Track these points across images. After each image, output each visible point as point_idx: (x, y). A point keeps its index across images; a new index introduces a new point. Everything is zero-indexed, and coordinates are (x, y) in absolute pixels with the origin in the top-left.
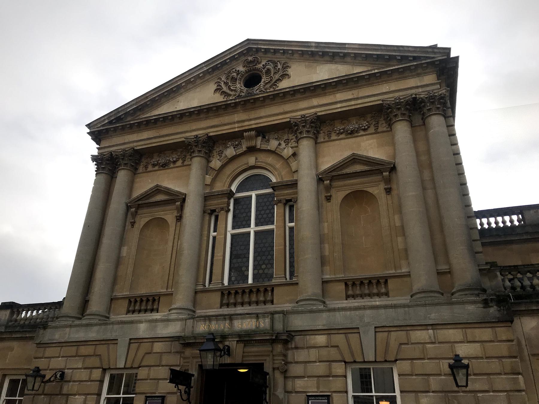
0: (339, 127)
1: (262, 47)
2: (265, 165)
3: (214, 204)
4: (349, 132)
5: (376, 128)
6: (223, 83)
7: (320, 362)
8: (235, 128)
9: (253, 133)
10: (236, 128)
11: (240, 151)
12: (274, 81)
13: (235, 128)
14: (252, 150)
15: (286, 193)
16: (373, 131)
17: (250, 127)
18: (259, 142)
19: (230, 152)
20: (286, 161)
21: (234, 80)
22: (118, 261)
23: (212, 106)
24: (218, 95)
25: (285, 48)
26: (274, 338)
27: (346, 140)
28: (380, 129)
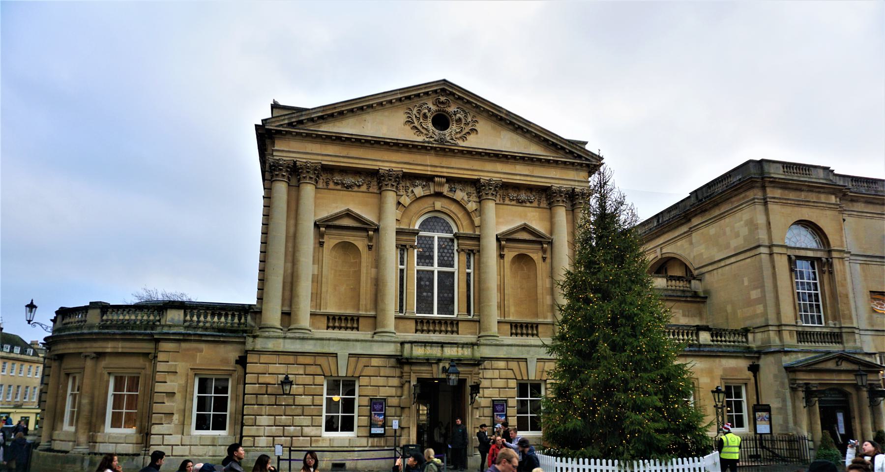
0: (513, 194)
1: (457, 93)
6: (414, 117)
8: (428, 171)
9: (444, 180)
10: (429, 171)
11: (427, 192)
12: (464, 132)
13: (428, 171)
14: (439, 195)
15: (469, 244)
16: (537, 206)
17: (442, 174)
18: (445, 190)
19: (419, 191)
20: (468, 214)
21: (425, 116)
23: (409, 143)
24: (408, 127)
25: (478, 104)
27: (517, 207)
28: (542, 205)
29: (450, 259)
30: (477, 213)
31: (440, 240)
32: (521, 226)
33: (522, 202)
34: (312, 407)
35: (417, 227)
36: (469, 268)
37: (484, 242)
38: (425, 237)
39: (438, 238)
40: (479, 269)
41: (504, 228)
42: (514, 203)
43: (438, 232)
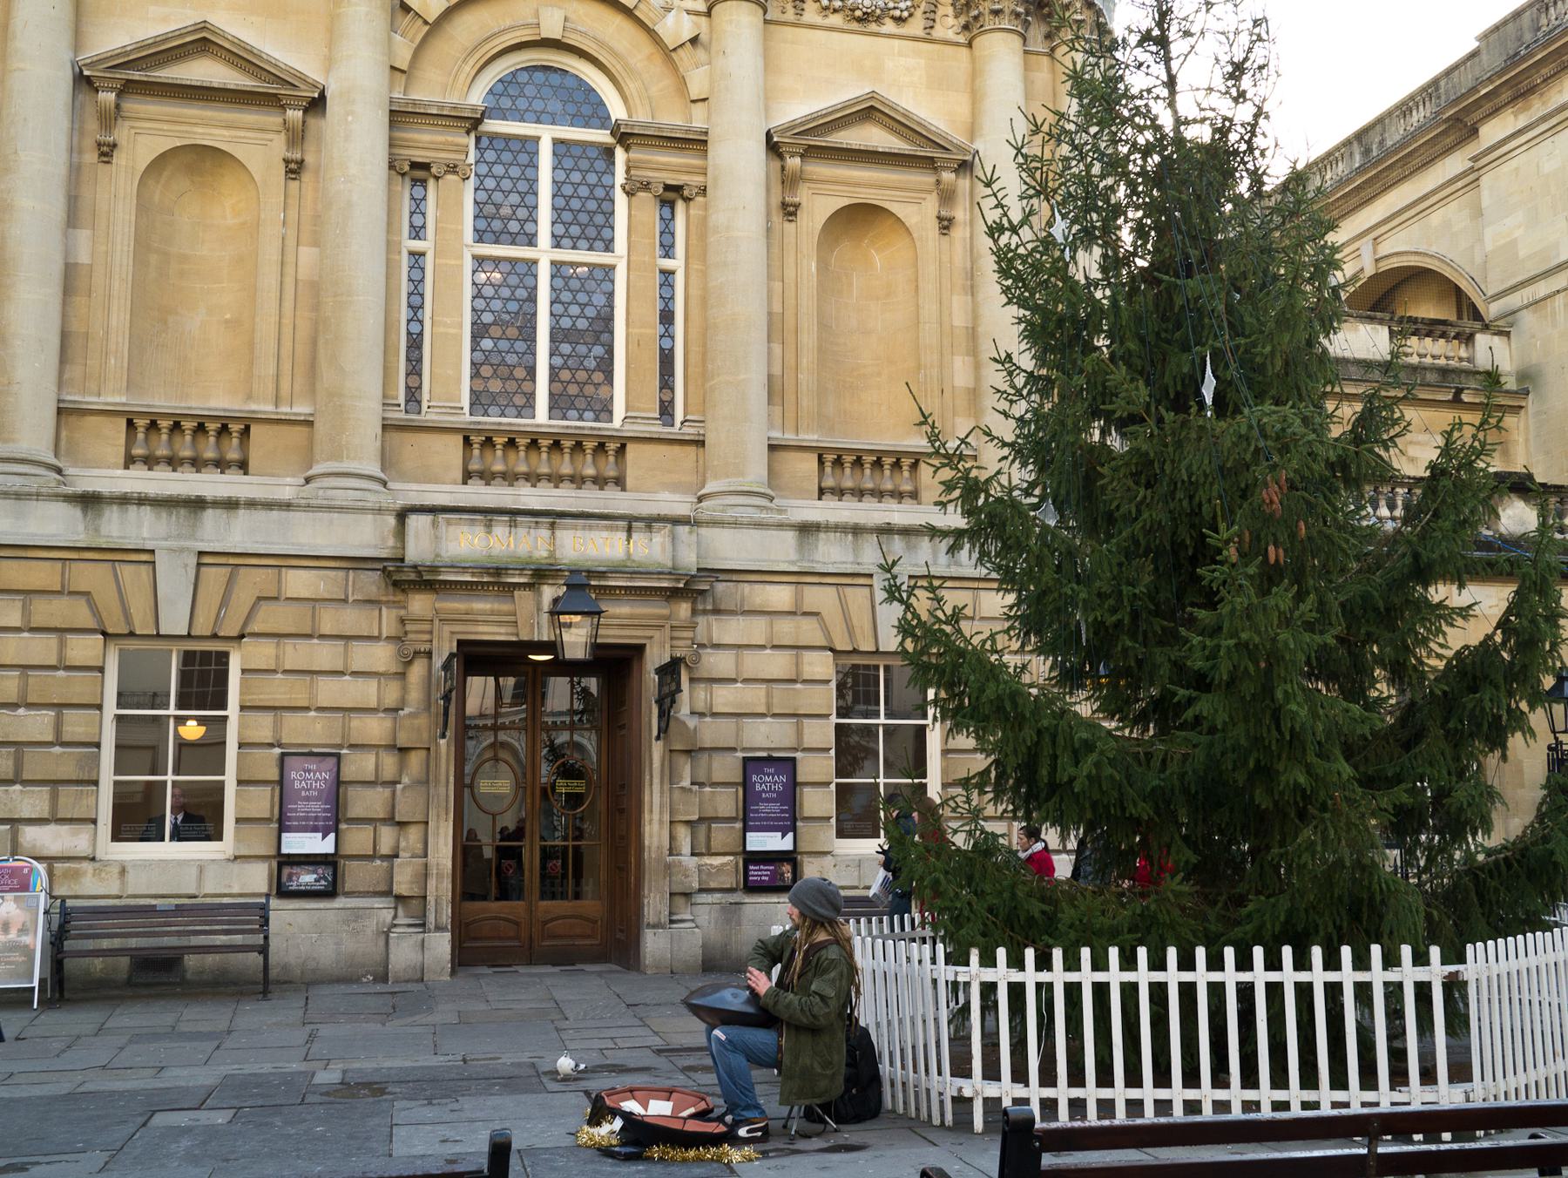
2: (594, 46)
3: (426, 143)
4: (858, 13)
5: (931, 23)
7: (774, 647)
15: (667, 165)
16: (920, 33)
20: (668, 53)
22: (71, 280)
26: (681, 585)
28: (939, 32)
29: (599, 219)
30: (700, 54)
31: (563, 149)
32: (858, 101)
33: (865, 18)
34: (57, 750)
35: (476, 97)
36: (668, 251)
37: (719, 153)
38: (508, 138)
39: (558, 143)
40: (704, 257)
41: (796, 108)
42: (836, 20)
43: (553, 123)
